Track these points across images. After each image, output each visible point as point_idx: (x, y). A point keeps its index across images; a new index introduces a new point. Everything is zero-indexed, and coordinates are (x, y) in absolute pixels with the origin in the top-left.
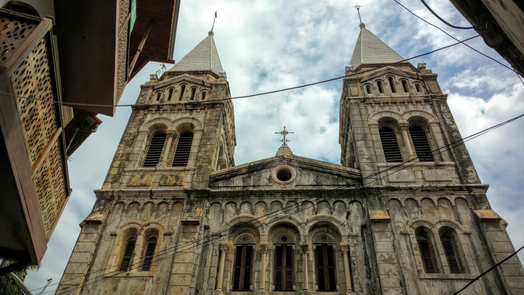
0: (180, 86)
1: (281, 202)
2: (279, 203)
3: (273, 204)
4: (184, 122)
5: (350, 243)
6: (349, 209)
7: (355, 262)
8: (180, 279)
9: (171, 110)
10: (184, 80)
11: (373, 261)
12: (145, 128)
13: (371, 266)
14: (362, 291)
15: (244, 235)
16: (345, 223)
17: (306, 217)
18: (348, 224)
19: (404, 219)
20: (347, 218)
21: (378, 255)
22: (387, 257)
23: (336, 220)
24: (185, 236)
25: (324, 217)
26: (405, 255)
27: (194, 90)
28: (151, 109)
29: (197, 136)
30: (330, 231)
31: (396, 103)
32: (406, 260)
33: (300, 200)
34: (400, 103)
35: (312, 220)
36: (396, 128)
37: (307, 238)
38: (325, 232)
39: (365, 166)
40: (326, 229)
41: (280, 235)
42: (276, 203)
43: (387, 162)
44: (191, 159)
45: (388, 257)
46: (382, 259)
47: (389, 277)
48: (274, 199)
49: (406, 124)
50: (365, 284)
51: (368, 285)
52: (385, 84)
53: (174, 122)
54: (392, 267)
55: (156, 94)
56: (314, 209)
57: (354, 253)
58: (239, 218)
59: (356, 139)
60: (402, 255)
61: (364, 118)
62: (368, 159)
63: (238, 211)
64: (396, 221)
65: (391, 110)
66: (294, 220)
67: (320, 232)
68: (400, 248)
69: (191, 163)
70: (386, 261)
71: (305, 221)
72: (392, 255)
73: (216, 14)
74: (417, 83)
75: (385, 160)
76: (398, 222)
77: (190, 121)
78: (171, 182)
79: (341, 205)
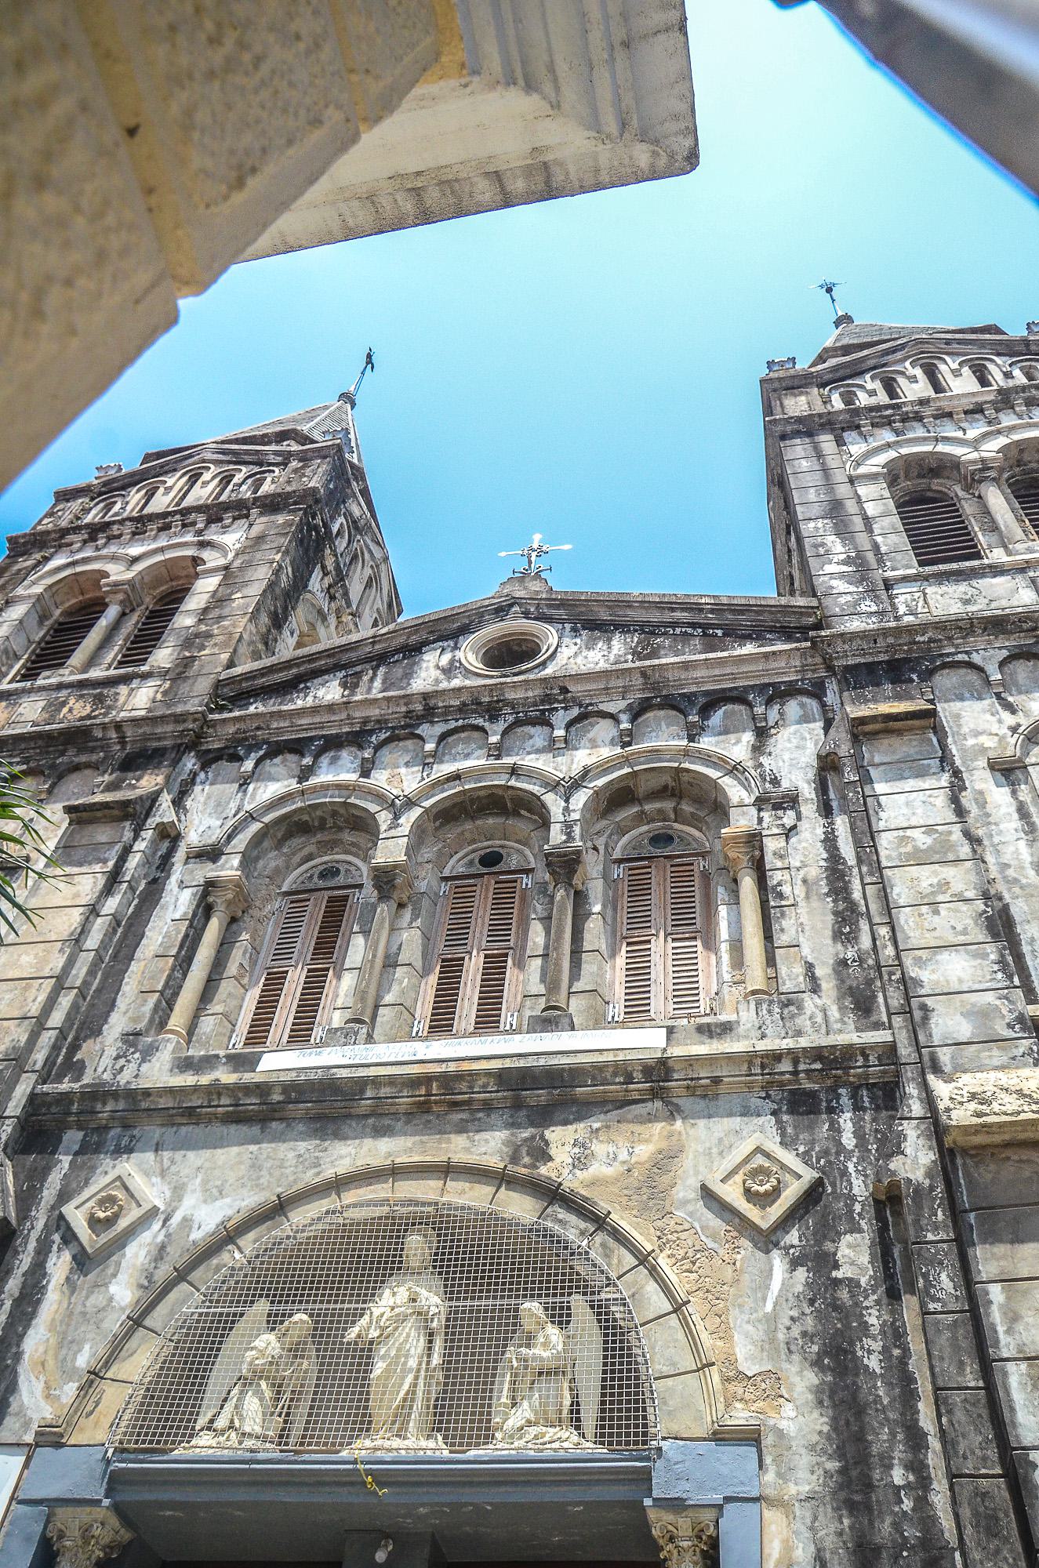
0: (186, 478)
1: (482, 730)
2: (476, 734)
3: (450, 739)
4: (167, 556)
5: (765, 825)
6: (766, 719)
7: (786, 889)
8: (8, 996)
9: (134, 534)
10: (204, 461)
11: (865, 869)
12: (34, 587)
13: (857, 895)
14: (815, 989)
15: (325, 863)
16: (749, 764)
17: (582, 758)
18: (761, 765)
19: (1000, 721)
20: (758, 749)
21: (885, 841)
22: (922, 840)
23: (708, 759)
24: (69, 855)
25: (655, 753)
26: (1010, 836)
27: (226, 480)
28: (70, 538)
29: (206, 586)
30: (687, 807)
31: (950, 415)
32: (1017, 852)
33: (562, 712)
34: (966, 412)
35: (604, 768)
36: (958, 489)
37: (577, 829)
38: (664, 820)
39: (834, 583)
40: (668, 805)
41: (474, 851)
42: (463, 735)
43: (921, 564)
44: (166, 645)
45: (929, 840)
46: (902, 850)
47: (936, 912)
48: (457, 720)
49: (994, 459)
50: (832, 962)
51: (843, 963)
52: (913, 379)
53: (135, 560)
54: (949, 872)
55: (102, 505)
56: (622, 733)
57: (781, 857)
58: (303, 792)
59: (800, 518)
60: (996, 840)
61: (832, 462)
62: (847, 562)
63: (305, 774)
64: (965, 730)
65: (932, 434)
66: (531, 774)
67: (641, 818)
68: (988, 815)
69: (163, 656)
70: (920, 859)
71: (576, 770)
72: (950, 833)
73: (369, 356)
74: (1028, 363)
75: (916, 565)
76: (977, 734)
77: (190, 552)
78: (75, 712)
79: (733, 712)
